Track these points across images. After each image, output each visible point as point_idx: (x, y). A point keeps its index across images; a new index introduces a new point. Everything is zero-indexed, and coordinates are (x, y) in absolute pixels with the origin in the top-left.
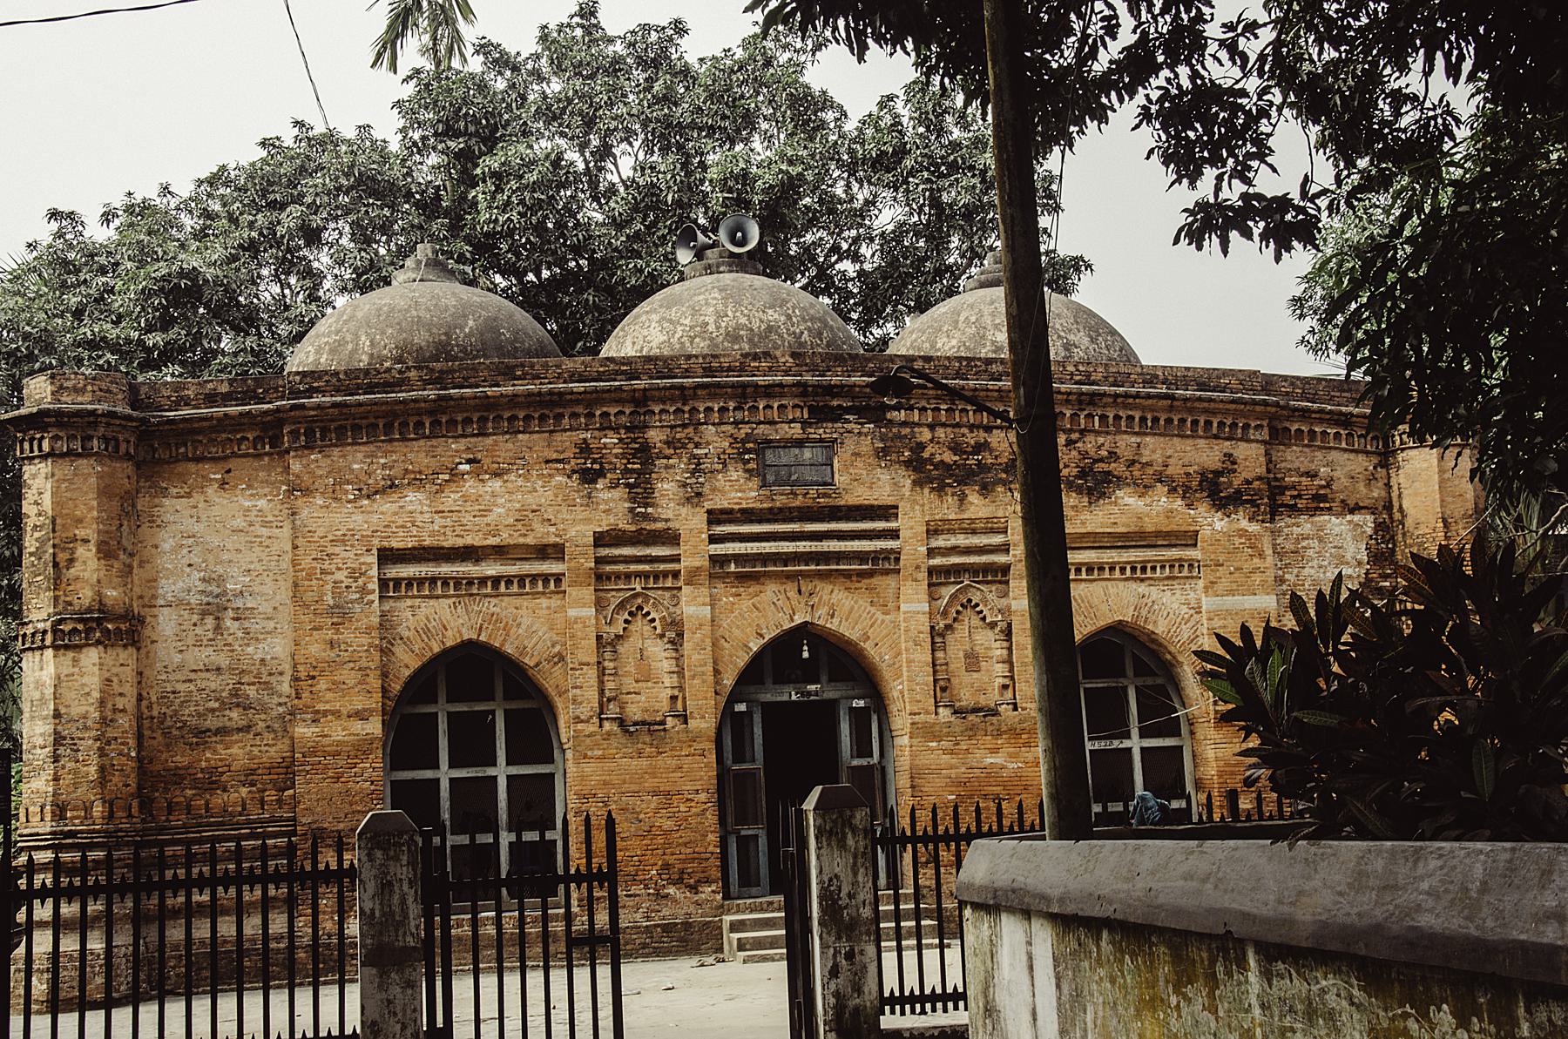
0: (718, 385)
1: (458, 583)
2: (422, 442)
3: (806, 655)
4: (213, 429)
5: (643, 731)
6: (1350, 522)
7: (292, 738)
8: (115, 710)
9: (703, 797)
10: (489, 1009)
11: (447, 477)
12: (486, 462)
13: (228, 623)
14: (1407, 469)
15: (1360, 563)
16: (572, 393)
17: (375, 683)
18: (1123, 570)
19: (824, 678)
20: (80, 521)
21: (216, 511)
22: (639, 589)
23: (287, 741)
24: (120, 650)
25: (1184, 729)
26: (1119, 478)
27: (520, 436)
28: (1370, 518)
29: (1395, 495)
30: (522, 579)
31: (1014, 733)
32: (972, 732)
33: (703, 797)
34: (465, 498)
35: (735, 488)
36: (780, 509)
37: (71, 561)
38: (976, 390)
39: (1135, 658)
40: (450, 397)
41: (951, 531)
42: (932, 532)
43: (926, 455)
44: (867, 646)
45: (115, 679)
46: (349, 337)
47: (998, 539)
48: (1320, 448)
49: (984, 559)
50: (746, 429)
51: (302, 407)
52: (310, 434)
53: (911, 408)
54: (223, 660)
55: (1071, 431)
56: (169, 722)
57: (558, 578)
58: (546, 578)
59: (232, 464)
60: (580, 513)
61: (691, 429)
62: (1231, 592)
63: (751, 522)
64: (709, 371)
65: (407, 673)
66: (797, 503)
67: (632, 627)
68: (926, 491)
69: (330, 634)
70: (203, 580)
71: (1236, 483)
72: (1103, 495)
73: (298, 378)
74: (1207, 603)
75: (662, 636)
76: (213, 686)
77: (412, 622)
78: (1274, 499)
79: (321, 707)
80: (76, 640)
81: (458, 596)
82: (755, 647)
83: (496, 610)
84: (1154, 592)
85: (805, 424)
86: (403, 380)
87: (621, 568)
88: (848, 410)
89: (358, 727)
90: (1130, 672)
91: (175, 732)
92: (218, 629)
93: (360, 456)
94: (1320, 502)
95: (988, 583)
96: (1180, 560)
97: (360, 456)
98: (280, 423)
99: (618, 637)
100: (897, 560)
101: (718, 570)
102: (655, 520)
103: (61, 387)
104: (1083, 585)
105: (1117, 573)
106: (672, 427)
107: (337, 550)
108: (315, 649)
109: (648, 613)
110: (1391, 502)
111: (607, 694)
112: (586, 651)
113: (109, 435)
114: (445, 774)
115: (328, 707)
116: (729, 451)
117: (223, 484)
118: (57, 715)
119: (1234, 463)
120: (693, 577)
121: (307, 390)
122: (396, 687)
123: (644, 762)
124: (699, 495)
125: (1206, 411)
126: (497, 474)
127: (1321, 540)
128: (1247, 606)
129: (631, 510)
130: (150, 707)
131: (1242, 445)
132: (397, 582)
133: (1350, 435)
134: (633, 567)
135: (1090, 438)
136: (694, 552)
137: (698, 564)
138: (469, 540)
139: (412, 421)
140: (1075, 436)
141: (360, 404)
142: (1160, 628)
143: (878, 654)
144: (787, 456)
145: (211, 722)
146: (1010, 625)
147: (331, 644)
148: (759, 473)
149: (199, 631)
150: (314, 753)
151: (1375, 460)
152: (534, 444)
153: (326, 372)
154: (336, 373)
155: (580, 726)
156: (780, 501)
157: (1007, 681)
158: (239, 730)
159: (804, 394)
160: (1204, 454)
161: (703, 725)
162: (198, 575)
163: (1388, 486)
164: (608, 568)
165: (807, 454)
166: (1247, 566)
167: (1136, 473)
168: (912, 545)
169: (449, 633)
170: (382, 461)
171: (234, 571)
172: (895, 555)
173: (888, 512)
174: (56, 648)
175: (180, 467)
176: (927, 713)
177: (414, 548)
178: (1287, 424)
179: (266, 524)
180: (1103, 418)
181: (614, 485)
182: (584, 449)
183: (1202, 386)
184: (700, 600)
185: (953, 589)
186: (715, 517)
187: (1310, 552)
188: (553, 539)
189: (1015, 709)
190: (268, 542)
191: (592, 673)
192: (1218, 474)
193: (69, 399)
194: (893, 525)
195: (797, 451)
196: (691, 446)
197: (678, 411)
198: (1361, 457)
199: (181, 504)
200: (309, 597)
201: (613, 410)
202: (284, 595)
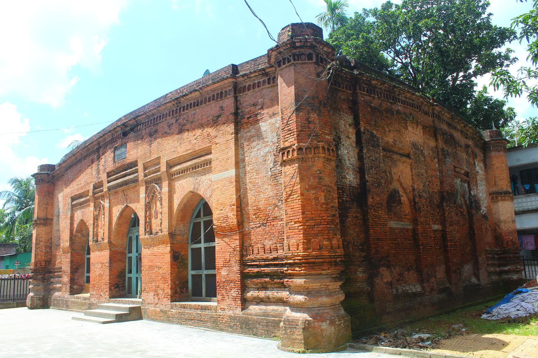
41: (151, 166)
62: (220, 171)
128: (226, 176)
131: (226, 100)
140: (177, 118)
192: (219, 116)
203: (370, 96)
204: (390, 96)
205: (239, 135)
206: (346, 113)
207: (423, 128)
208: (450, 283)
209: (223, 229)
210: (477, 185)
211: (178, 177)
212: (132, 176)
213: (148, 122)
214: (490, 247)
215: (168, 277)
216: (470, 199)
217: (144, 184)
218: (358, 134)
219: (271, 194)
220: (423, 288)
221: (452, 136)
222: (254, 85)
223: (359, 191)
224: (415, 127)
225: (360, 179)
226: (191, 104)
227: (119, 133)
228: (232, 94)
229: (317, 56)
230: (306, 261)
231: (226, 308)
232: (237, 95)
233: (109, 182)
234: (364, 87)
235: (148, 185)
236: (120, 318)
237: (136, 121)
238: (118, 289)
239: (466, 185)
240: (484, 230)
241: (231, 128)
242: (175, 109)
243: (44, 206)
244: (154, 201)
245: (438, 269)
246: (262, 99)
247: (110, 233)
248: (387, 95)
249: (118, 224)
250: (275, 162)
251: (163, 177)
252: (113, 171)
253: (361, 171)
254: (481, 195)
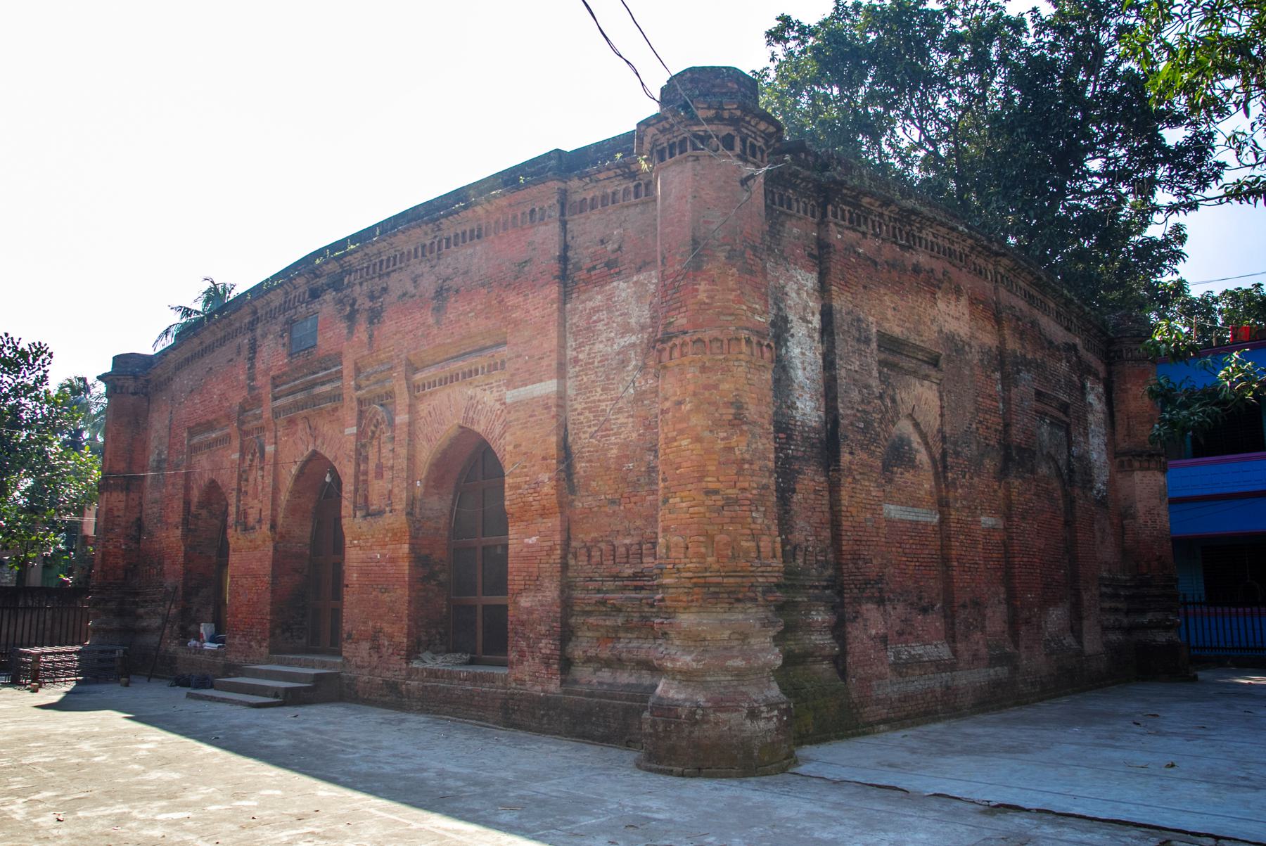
6: (636, 283)
94: (612, 268)
127: (609, 309)
128: (536, 394)
131: (543, 228)
140: (434, 263)
187: (600, 326)
191: (234, 493)
203: (855, 230)
204: (901, 231)
205: (568, 306)
206: (803, 267)
207: (971, 303)
208: (1017, 646)
209: (525, 507)
210: (1087, 435)
211: (431, 394)
212: (327, 388)
213: (368, 268)
214: (1109, 571)
215: (404, 610)
216: (1069, 463)
217: (355, 404)
218: (827, 314)
220: (955, 652)
221: (1034, 324)
222: (604, 197)
223: (823, 435)
224: (953, 303)
225: (827, 412)
226: (464, 233)
227: (301, 290)
228: (556, 214)
229: (743, 141)
230: (702, 580)
231: (527, 678)
232: (567, 218)
233: (275, 398)
234: (843, 211)
235: (364, 408)
236: (292, 698)
237: (341, 266)
238: (287, 635)
239: (1062, 434)
240: (1098, 534)
241: (553, 291)
242: (428, 243)
244: (375, 442)
245: (989, 612)
247: (274, 509)
248: (894, 228)
249: (296, 492)
251: (397, 392)
253: (829, 392)
254: (1095, 456)
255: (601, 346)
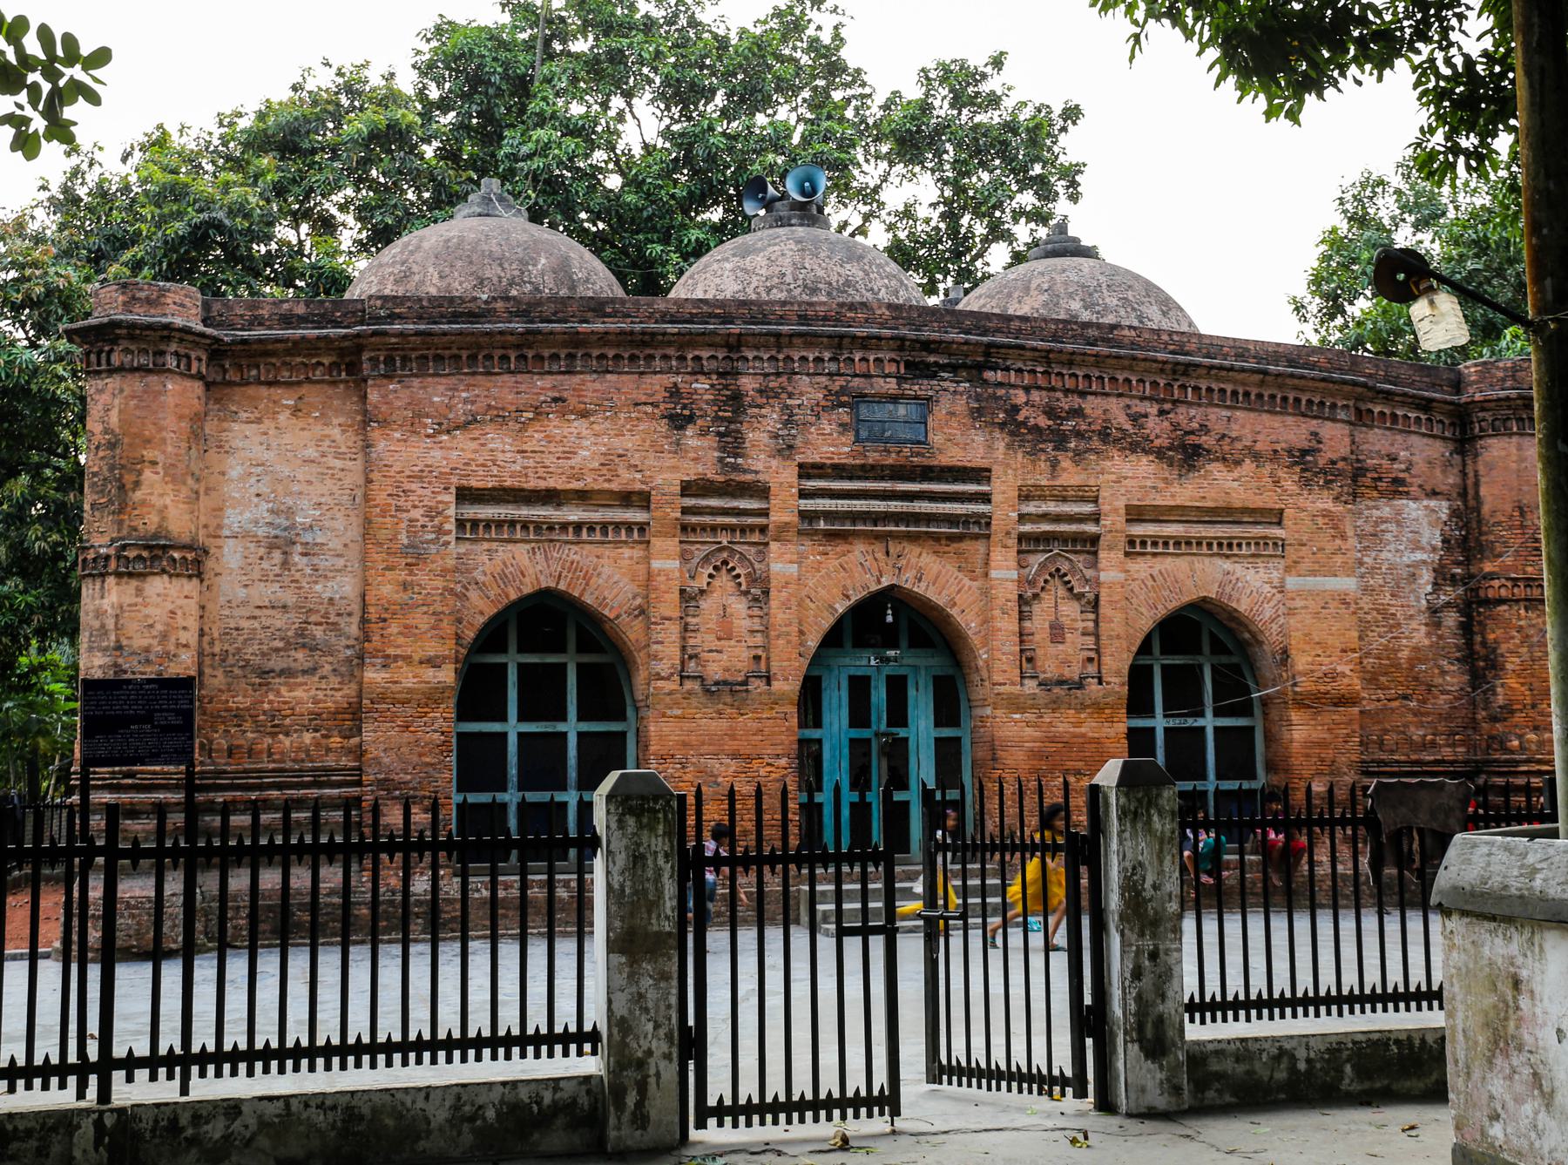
0: (815, 335)
1: (538, 527)
2: (506, 377)
3: (890, 619)
4: (288, 352)
5: (728, 691)
6: (1426, 507)
7: (361, 684)
8: (178, 645)
9: (783, 762)
10: (998, 1040)
11: (531, 415)
12: (573, 401)
13: (297, 558)
14: (1486, 456)
15: (1434, 549)
16: (664, 334)
17: (448, 628)
18: (1210, 545)
19: (904, 643)
20: (149, 441)
21: (287, 438)
22: (725, 543)
23: (354, 686)
24: (184, 581)
25: (1257, 711)
26: (1208, 451)
27: (609, 376)
28: (1445, 504)
29: (1470, 482)
30: (604, 526)
31: (1097, 707)
32: (1055, 705)
33: (783, 762)
34: (549, 439)
35: (828, 442)
36: (873, 467)
37: (137, 484)
38: (1073, 353)
39: (1212, 635)
40: (539, 332)
41: (1042, 498)
42: (1025, 497)
43: (1020, 418)
44: (954, 612)
45: (179, 612)
46: (415, 268)
47: (1088, 508)
48: (1401, 431)
49: (1074, 528)
50: (840, 382)
51: (384, 333)
52: (390, 361)
53: (1007, 369)
54: (289, 598)
55: (1164, 400)
56: (231, 660)
57: (642, 528)
58: (629, 526)
59: (304, 390)
60: (669, 461)
61: (784, 379)
62: (1313, 573)
63: (842, 478)
64: (803, 319)
65: (481, 620)
66: (890, 461)
67: (716, 583)
68: (1020, 456)
69: (403, 575)
70: (272, 511)
71: (1321, 463)
72: (1192, 468)
73: (379, 303)
74: (1292, 582)
75: (746, 593)
76: (278, 624)
77: (488, 567)
78: (1358, 480)
79: (391, 651)
80: (139, 567)
81: (537, 541)
82: (841, 609)
83: (577, 558)
84: (1238, 569)
85: (900, 379)
86: (489, 311)
87: (707, 519)
88: (943, 367)
89: (429, 674)
90: (1206, 648)
91: (237, 671)
92: (285, 564)
93: (441, 388)
94: (1397, 488)
95: (1076, 552)
96: (1265, 538)
97: (441, 388)
98: (359, 349)
99: (702, 592)
100: (988, 524)
101: (806, 526)
102: (745, 471)
103: (134, 298)
104: (1169, 559)
105: (1205, 550)
106: (766, 375)
107: (414, 486)
108: (386, 589)
109: (733, 569)
110: (1465, 488)
111: (690, 651)
112: (669, 605)
113: (182, 351)
114: (572, 727)
115: (399, 652)
116: (823, 403)
117: (296, 411)
118: (119, 647)
119: (1320, 442)
120: (782, 533)
121: (389, 316)
122: (470, 635)
123: (724, 724)
124: (790, 447)
125: (1296, 388)
126: (584, 414)
127: (1399, 523)
129: (721, 460)
130: (212, 643)
131: (1329, 424)
132: (475, 523)
133: (1429, 420)
134: (720, 520)
135: (1182, 409)
136: (784, 509)
137: (787, 519)
138: (551, 483)
139: (498, 353)
140: (1167, 406)
141: (445, 334)
142: (1243, 606)
143: (967, 619)
144: (881, 412)
145: (276, 663)
146: (1097, 597)
147: (405, 586)
148: (853, 427)
149: (265, 565)
150: (382, 698)
151: (1451, 446)
152: (623, 385)
153: (409, 299)
154: (420, 300)
155: (660, 683)
156: (873, 457)
157: (1092, 654)
158: (304, 672)
159: (901, 348)
160: (1291, 431)
161: (786, 688)
162: (265, 506)
163: (1464, 473)
164: (694, 519)
165: (902, 410)
166: (1329, 547)
167: (1226, 448)
168: (1004, 511)
169: (527, 580)
170: (464, 395)
171: (304, 503)
172: (985, 521)
173: (980, 474)
174: (119, 575)
175: (251, 391)
176: (1013, 684)
177: (494, 489)
178: (1370, 406)
179: (339, 456)
180: (1196, 389)
181: (703, 433)
182: (674, 393)
183: (1292, 363)
184: (787, 557)
185: (1042, 558)
186: (806, 471)
187: (1388, 536)
188: (638, 486)
189: (1100, 683)
190: (341, 475)
191: (674, 629)
192: (1304, 452)
193: (141, 311)
194: (985, 488)
195: (891, 407)
196: (784, 396)
197: (772, 358)
198: (1438, 444)
199: (250, 429)
200: (383, 535)
201: (705, 354)
202: (354, 533)
217: (1013, 542)
219: (1427, 642)
242: (1162, 383)
243: (190, 481)
246: (1407, 454)
250: (1435, 584)
252: (835, 467)
255: (1390, 555)
